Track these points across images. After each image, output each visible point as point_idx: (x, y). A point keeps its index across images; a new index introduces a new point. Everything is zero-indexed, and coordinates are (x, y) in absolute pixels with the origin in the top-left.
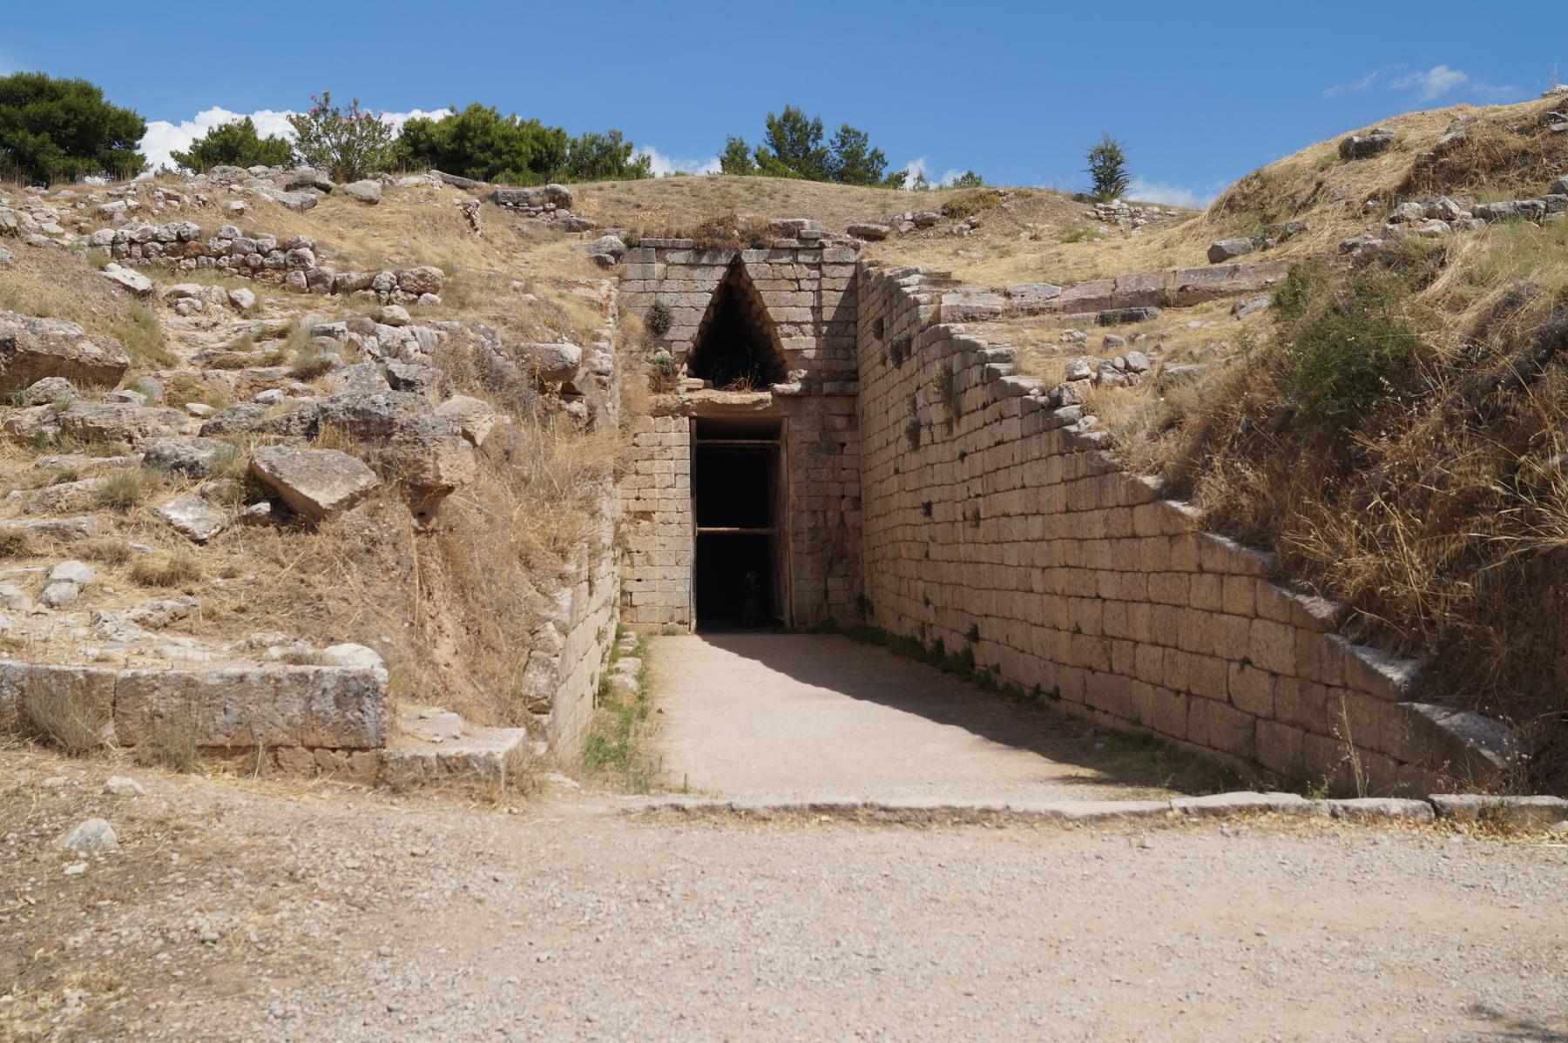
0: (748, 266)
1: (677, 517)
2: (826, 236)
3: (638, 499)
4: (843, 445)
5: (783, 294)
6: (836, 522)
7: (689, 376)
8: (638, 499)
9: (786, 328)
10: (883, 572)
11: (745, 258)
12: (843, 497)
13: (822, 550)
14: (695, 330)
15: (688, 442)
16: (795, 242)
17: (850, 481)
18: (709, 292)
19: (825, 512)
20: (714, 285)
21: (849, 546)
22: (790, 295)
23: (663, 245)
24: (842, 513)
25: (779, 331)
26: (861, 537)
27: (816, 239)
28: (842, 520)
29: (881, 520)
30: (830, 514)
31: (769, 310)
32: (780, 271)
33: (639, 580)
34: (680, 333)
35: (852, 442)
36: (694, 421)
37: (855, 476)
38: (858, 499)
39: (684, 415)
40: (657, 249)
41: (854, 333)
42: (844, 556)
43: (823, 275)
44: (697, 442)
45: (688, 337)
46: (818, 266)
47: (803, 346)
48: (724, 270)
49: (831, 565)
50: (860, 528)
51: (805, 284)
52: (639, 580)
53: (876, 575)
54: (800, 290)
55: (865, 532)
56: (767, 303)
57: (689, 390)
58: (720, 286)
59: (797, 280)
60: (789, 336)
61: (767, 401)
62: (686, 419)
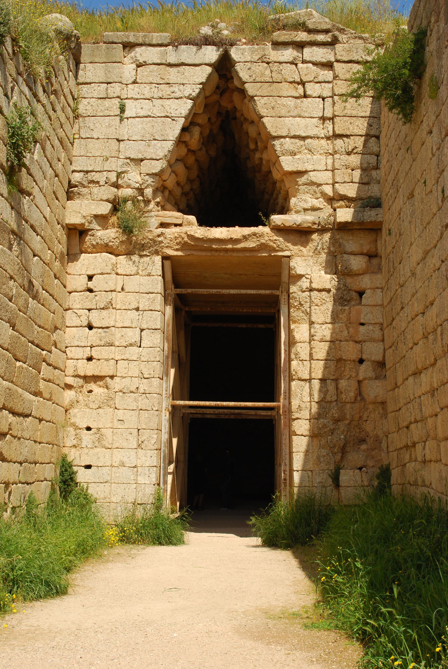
0: (238, 67)
1: (144, 386)
2: (341, 31)
3: (90, 359)
4: (361, 294)
5: (284, 100)
6: (352, 394)
7: (163, 208)
8: (90, 359)
9: (288, 143)
10: (424, 462)
11: (234, 53)
12: (361, 361)
13: (332, 432)
14: (169, 145)
15: (159, 287)
16: (303, 36)
17: (373, 340)
18: (188, 98)
19: (336, 380)
20: (195, 90)
21: (368, 427)
22: (291, 102)
23: (132, 39)
24: (359, 382)
25: (278, 148)
26: (385, 415)
27: (327, 31)
28: (360, 393)
29: (424, 378)
30: (343, 383)
31: (265, 120)
32: (280, 72)
33: (88, 467)
34: (151, 150)
35: (374, 289)
36: (168, 263)
37: (377, 334)
38: (382, 364)
39: (157, 253)
40: (125, 47)
41: (376, 149)
42: (363, 441)
43: (336, 77)
44: (173, 291)
45: (161, 154)
46: (329, 65)
47: (309, 168)
48: (209, 70)
49: (343, 451)
50: (383, 403)
51: (311, 89)
52: (88, 467)
53: (411, 466)
54: (305, 96)
55: (391, 407)
56: (263, 111)
57: (163, 225)
58: (202, 90)
59: (302, 83)
60: (293, 154)
61: (262, 235)
62: (158, 259)
